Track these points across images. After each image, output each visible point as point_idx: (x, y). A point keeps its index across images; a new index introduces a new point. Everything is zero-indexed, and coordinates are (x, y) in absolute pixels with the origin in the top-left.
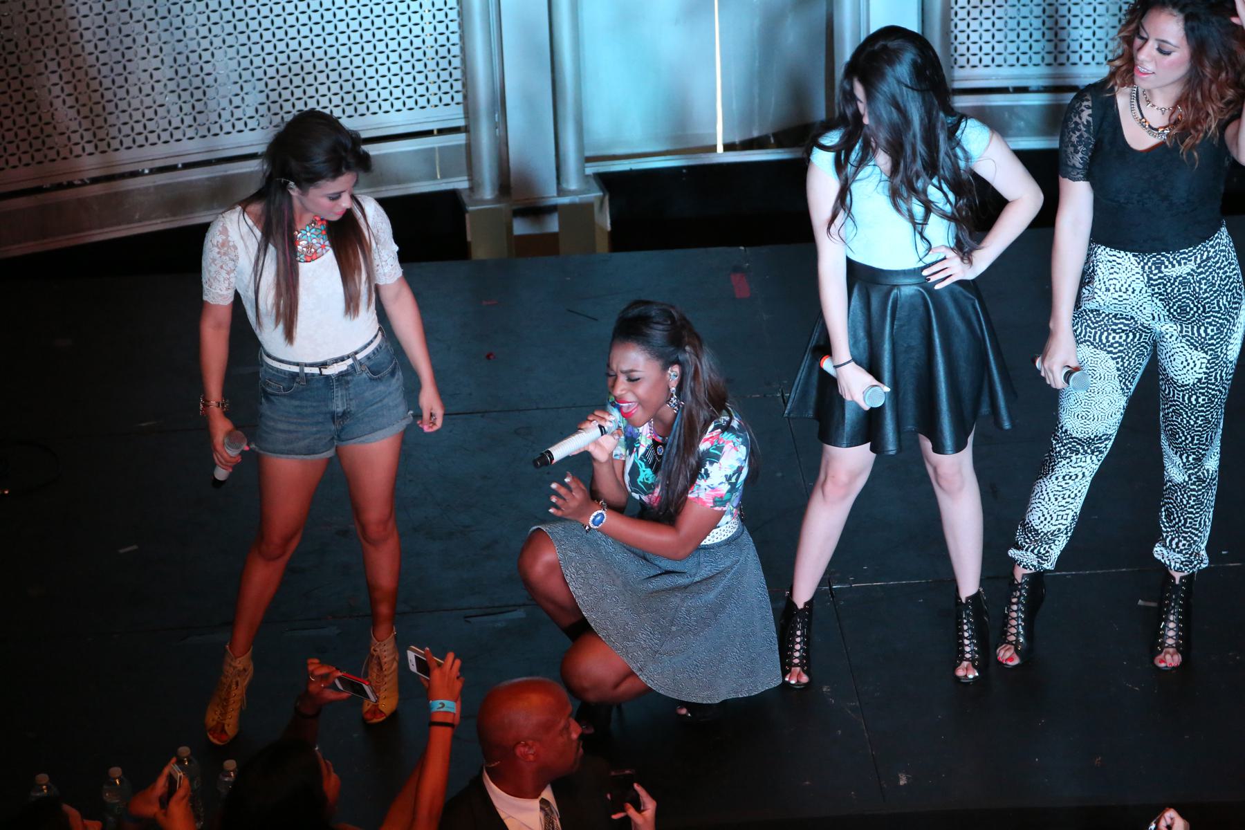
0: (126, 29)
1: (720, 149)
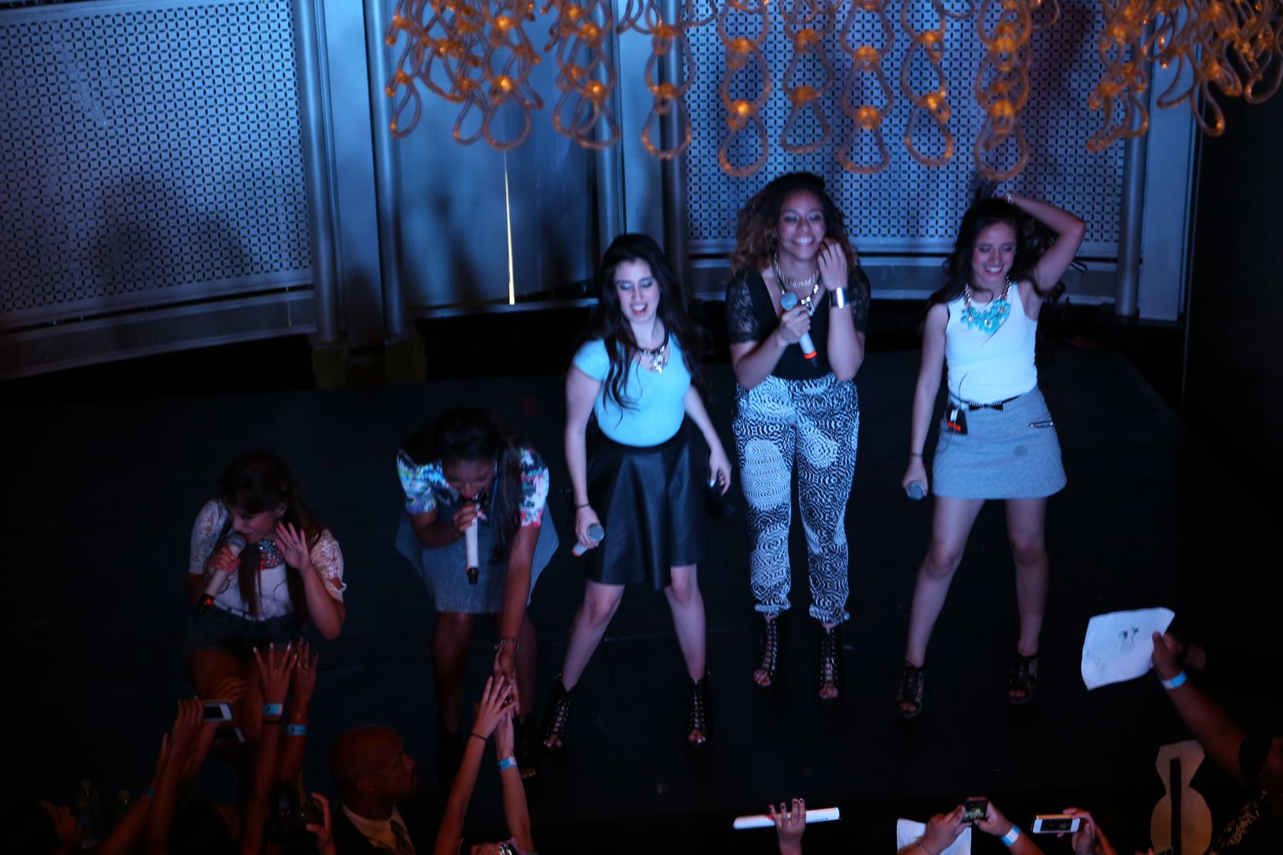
0: (38, 212)
1: (512, 301)
